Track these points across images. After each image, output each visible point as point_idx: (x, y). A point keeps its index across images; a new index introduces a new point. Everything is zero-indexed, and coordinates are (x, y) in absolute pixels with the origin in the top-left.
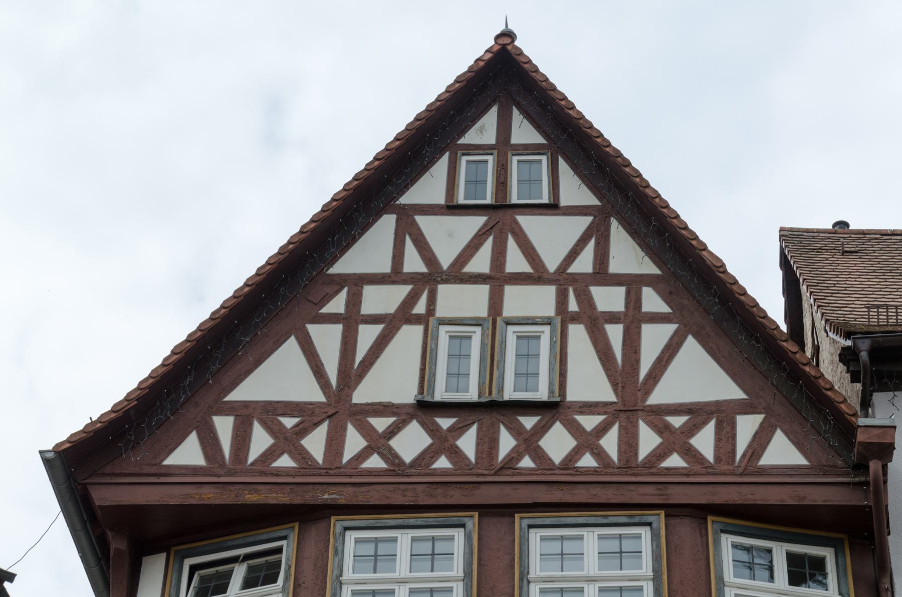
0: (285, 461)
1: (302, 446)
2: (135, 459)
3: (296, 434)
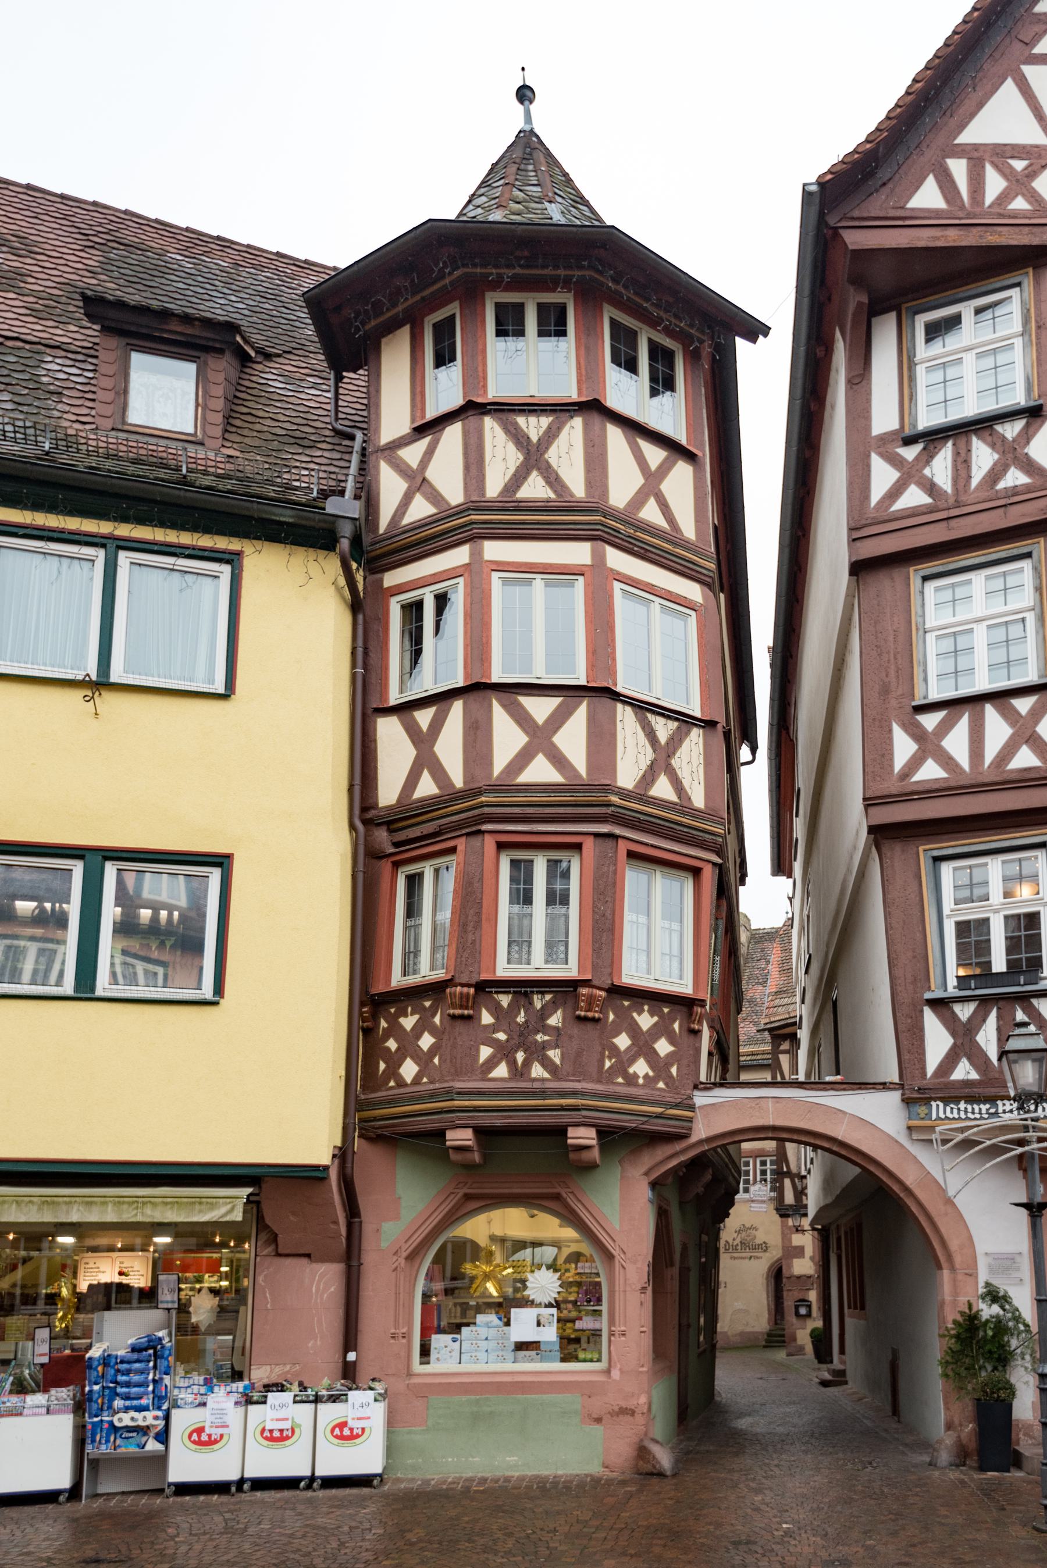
0: (1020, 204)
1: (1033, 188)
2: (877, 205)
3: (1027, 176)
